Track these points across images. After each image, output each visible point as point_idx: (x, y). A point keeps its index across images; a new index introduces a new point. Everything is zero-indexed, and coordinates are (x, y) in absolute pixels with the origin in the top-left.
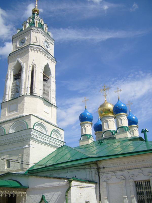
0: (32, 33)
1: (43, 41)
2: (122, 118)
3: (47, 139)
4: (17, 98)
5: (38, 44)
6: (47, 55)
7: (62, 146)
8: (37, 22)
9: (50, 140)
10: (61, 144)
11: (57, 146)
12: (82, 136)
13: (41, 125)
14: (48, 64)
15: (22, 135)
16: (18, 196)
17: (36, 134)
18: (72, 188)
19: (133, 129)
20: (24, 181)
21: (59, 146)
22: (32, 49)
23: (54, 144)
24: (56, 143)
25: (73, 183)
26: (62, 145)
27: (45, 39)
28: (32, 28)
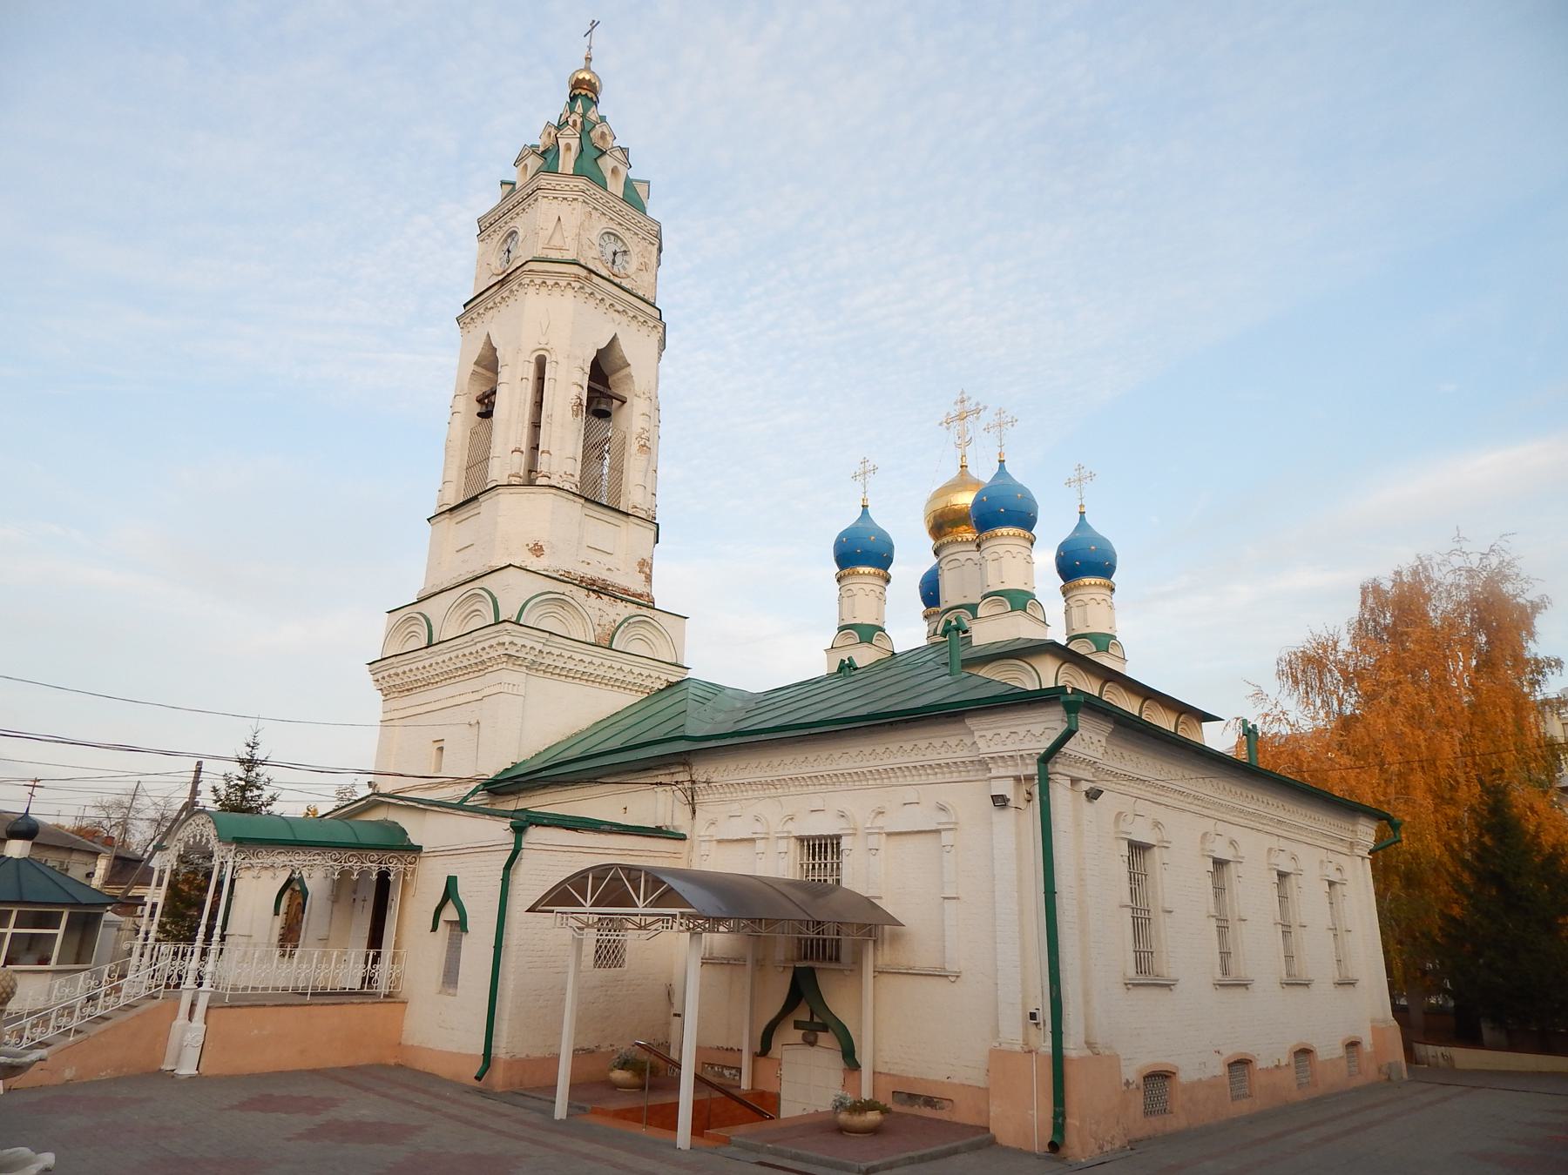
0: (543, 203)
1: (595, 236)
2: (1001, 550)
3: (587, 659)
4: (475, 498)
5: (568, 256)
6: (608, 302)
7: (670, 685)
8: (568, 147)
9: (608, 663)
10: (664, 677)
11: (648, 682)
12: (841, 629)
13: (561, 601)
14: (615, 338)
15: (479, 646)
16: (391, 878)
17: (529, 644)
18: (524, 854)
19: (1086, 598)
20: (418, 829)
21: (659, 685)
22: (538, 281)
23: (630, 678)
24: (636, 671)
25: (534, 835)
26: (674, 679)
27: (601, 224)
28: (543, 183)
